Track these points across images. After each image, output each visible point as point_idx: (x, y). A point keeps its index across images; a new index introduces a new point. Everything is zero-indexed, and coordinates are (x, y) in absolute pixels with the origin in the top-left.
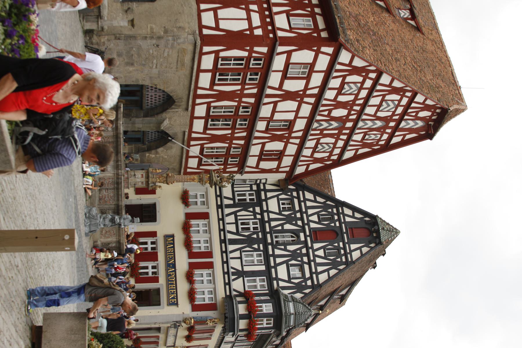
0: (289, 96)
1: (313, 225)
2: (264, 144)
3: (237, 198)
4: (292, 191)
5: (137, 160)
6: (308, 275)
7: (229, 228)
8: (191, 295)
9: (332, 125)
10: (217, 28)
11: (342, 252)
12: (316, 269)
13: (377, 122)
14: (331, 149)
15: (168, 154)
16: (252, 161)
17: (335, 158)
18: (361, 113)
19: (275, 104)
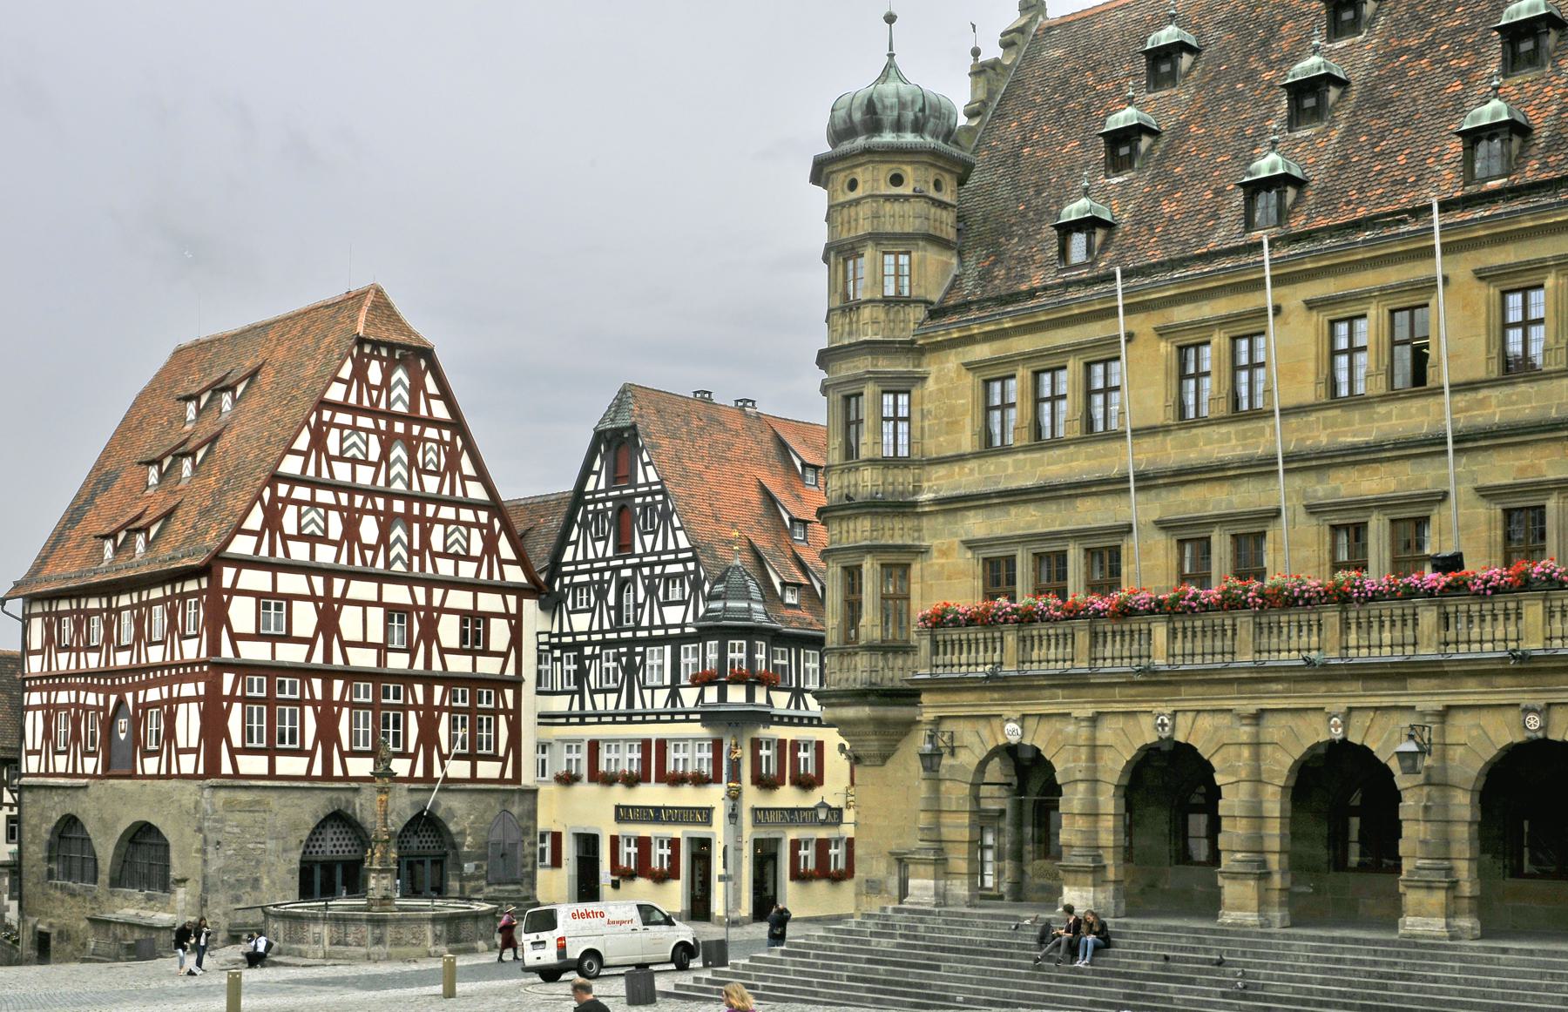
0: (328, 623)
1: (610, 553)
2: (443, 651)
3: (573, 687)
4: (562, 586)
5: (477, 867)
6: (679, 568)
7: (611, 707)
8: (699, 780)
9: (398, 539)
10: (196, 751)
11: (649, 499)
12: (671, 552)
13: (393, 457)
14: (463, 529)
15: (461, 815)
16: (489, 666)
17: (483, 516)
18: (369, 493)
19: (344, 645)
